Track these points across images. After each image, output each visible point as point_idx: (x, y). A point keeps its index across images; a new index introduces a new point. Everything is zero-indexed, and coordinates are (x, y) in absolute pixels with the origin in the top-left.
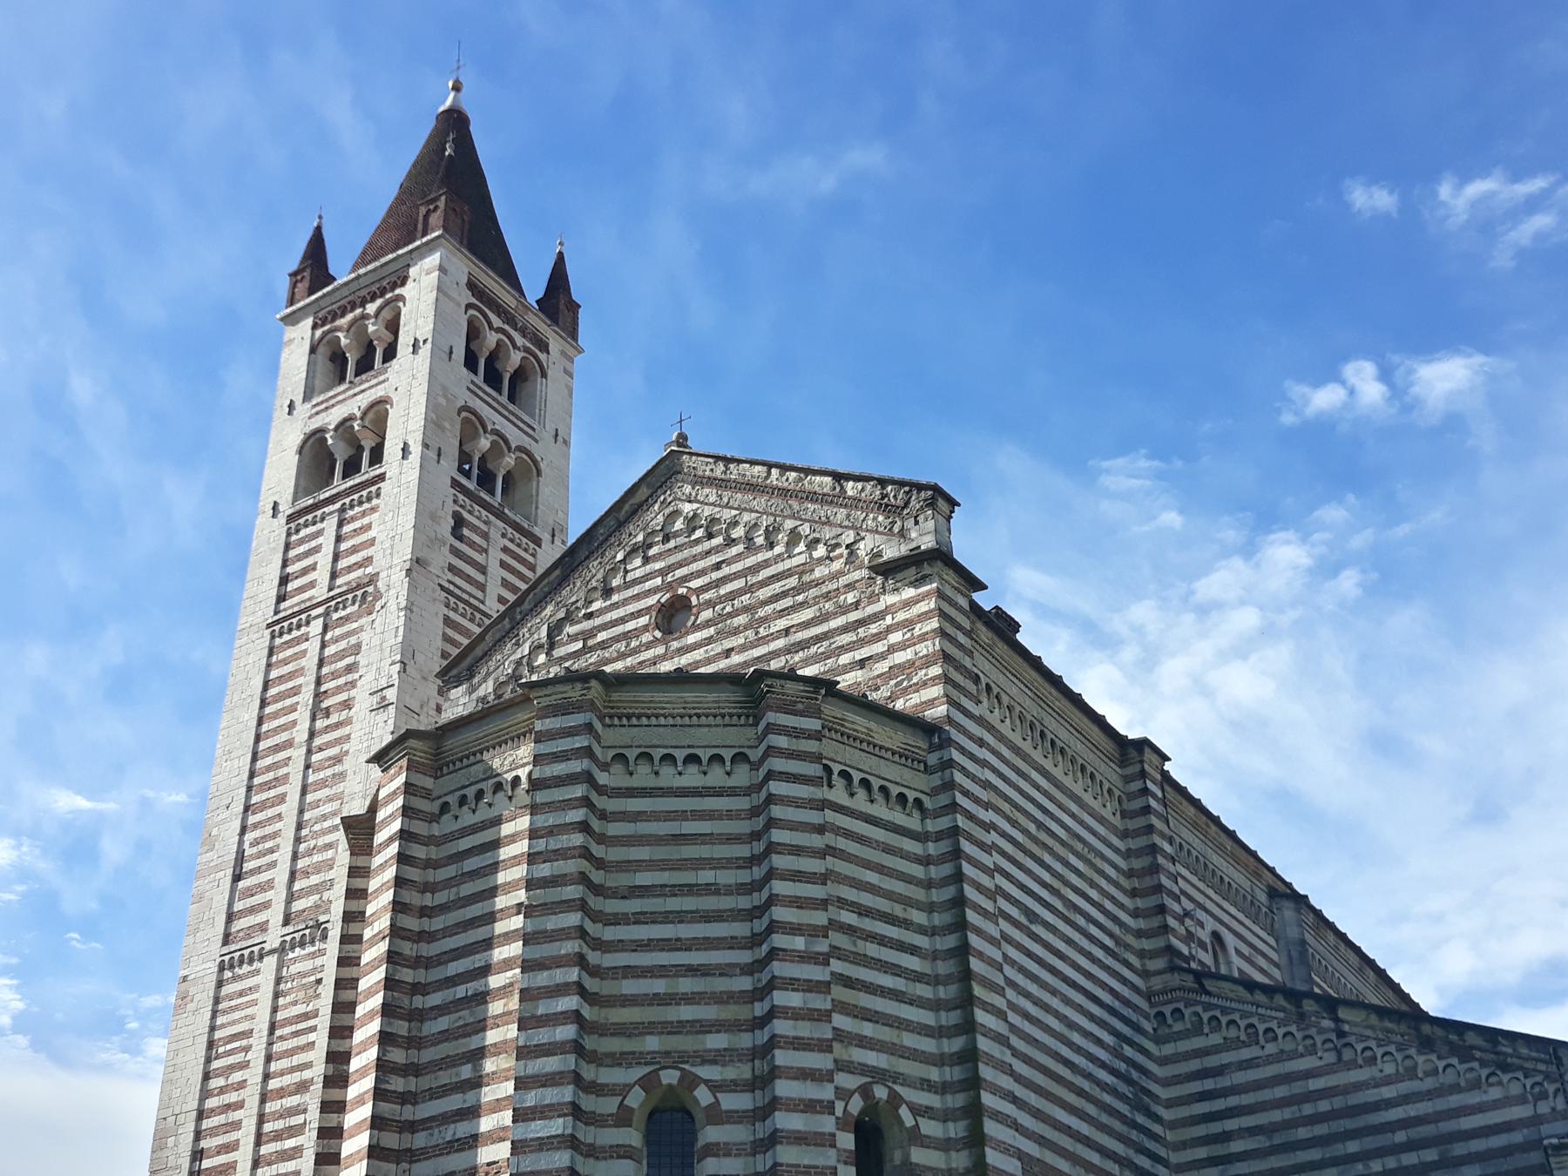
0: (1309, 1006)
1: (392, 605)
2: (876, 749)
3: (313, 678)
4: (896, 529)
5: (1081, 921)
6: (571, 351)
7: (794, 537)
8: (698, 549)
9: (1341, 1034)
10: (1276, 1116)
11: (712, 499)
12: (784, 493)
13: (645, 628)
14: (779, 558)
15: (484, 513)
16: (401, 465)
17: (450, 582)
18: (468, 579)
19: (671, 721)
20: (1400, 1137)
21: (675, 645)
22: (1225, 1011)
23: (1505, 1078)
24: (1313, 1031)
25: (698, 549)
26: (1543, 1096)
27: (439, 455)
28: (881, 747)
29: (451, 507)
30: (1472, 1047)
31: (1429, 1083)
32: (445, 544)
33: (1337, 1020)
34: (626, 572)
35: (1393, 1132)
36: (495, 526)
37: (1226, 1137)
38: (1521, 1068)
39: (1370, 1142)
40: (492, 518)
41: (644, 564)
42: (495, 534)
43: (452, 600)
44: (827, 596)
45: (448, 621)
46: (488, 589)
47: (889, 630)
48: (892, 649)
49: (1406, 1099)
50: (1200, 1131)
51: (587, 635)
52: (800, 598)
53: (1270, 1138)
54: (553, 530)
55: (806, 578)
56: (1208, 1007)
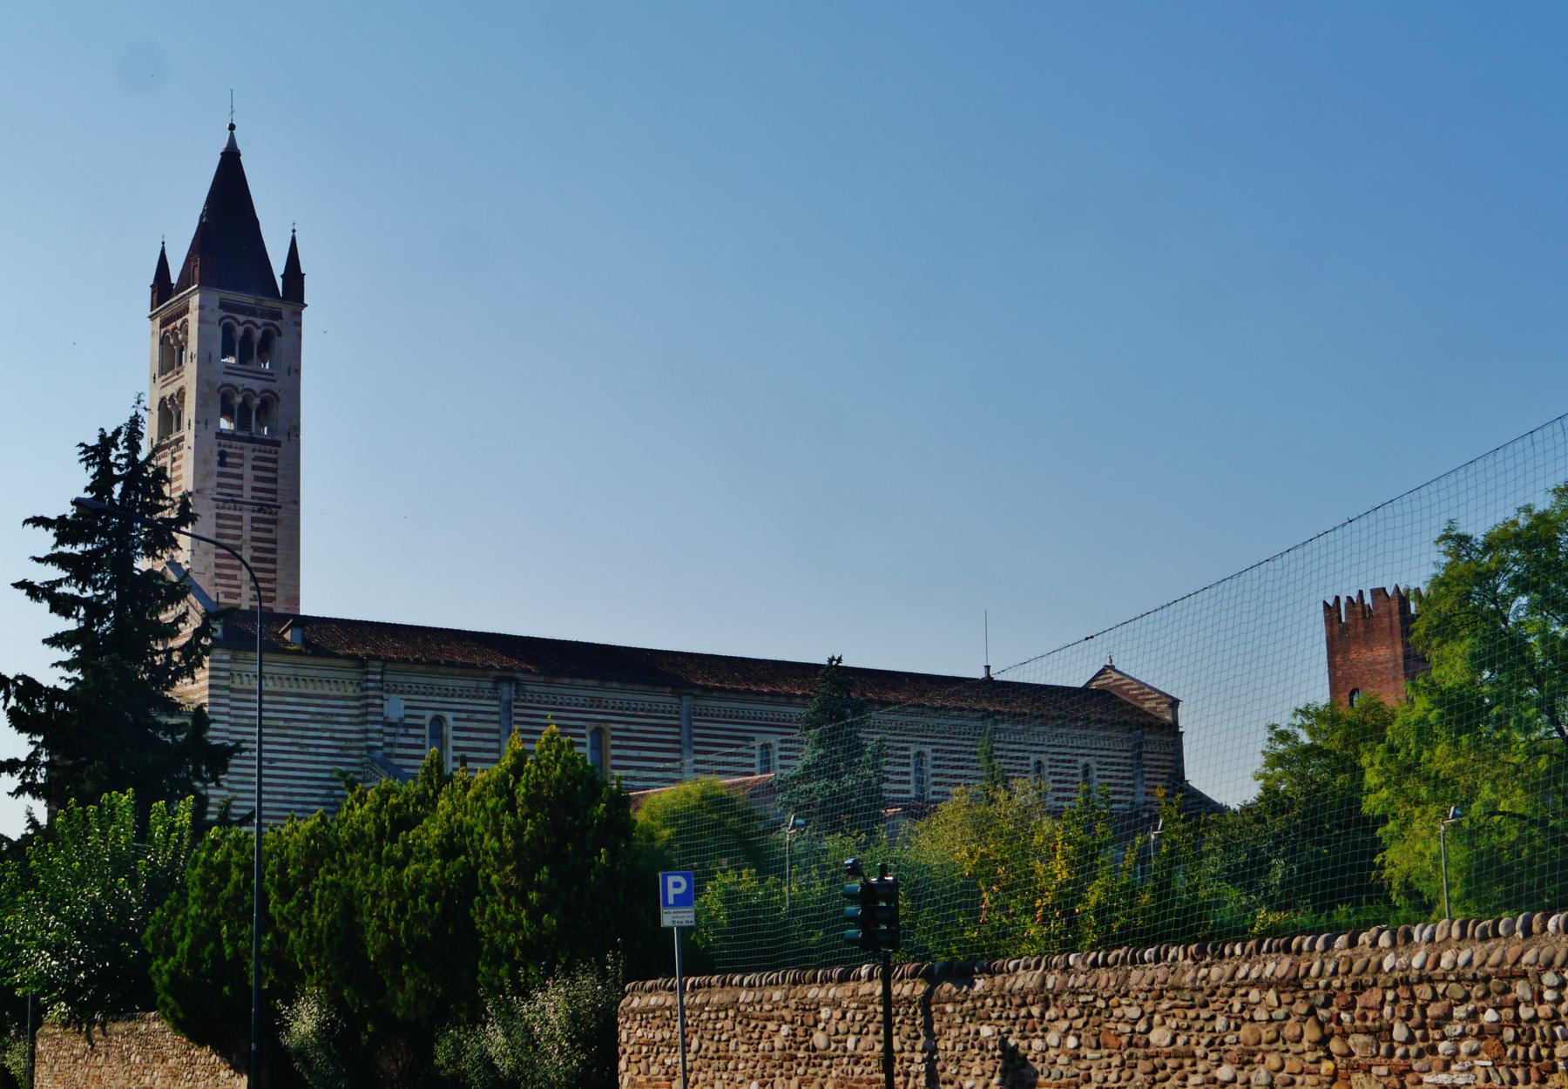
17: (218, 494)
27: (206, 424)
29: (216, 449)
40: (245, 444)
43: (221, 504)
45: (219, 516)
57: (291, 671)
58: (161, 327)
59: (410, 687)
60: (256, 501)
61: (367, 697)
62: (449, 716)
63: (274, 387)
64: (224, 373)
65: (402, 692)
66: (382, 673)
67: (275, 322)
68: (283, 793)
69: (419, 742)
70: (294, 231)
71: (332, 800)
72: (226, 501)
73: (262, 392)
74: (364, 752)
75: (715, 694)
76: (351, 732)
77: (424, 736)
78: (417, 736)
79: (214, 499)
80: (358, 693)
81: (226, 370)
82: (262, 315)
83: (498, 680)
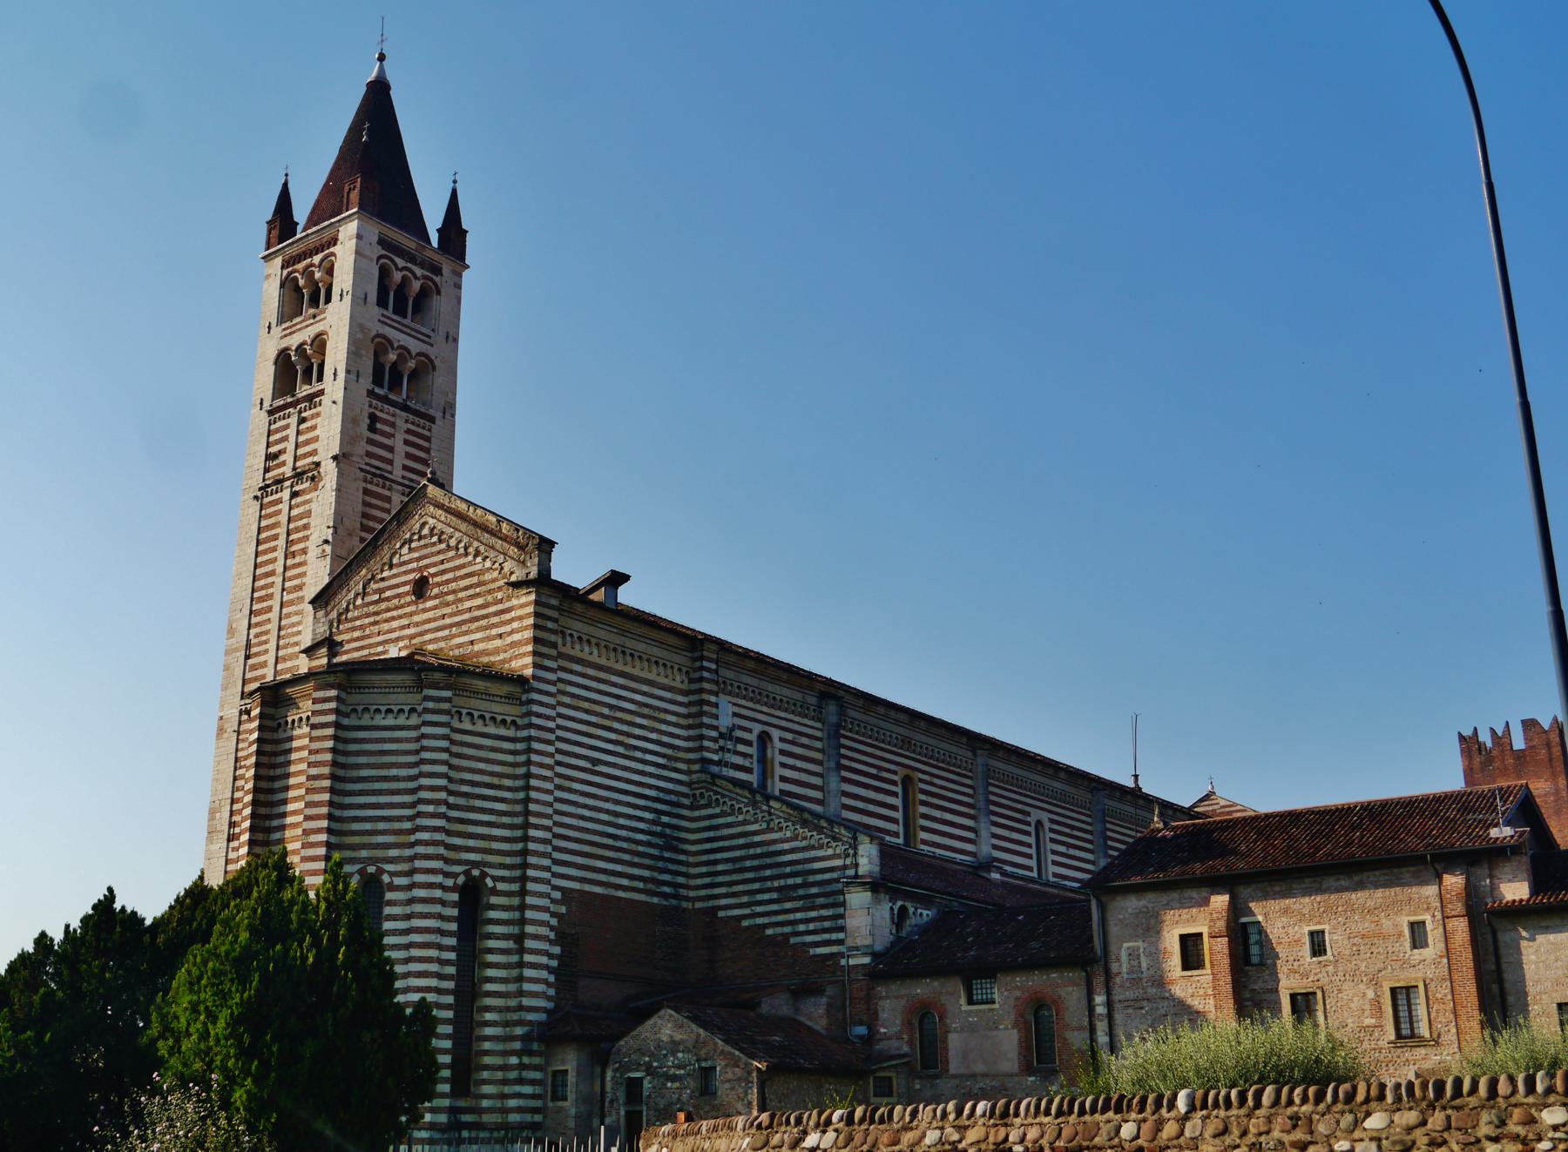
0: (758, 798)
1: (328, 486)
2: (490, 697)
3: (284, 530)
4: (522, 559)
5: (639, 755)
6: (458, 268)
7: (477, 554)
8: (435, 549)
9: (770, 814)
10: (738, 853)
11: (443, 519)
12: (475, 524)
13: (407, 593)
14: (470, 564)
15: (392, 409)
16: (333, 385)
17: (367, 464)
18: (381, 459)
19: (379, 690)
20: (788, 870)
21: (421, 606)
22: (723, 796)
23: (834, 844)
24: (758, 811)
25: (435, 549)
26: (847, 856)
27: (358, 376)
28: (493, 695)
29: (367, 410)
30: (823, 827)
31: (804, 843)
32: (363, 439)
33: (769, 806)
34: (401, 555)
35: (786, 867)
36: (400, 417)
37: (716, 862)
38: (841, 840)
39: (775, 871)
40: (398, 411)
41: (409, 553)
42: (400, 423)
43: (369, 476)
44: (489, 592)
45: (366, 492)
46: (395, 464)
47: (513, 620)
48: (512, 632)
49: (793, 851)
50: (705, 858)
51: (381, 591)
52: (478, 590)
53: (734, 865)
54: (444, 408)
55: (482, 578)
56: (716, 793)
57: (618, 640)
58: (282, 268)
59: (739, 687)
60: (407, 482)
61: (702, 691)
62: (776, 734)
63: (432, 352)
64: (379, 321)
65: (730, 694)
66: (717, 662)
67: (434, 277)
68: (607, 812)
69: (747, 764)
70: (455, 182)
71: (659, 829)
72: (374, 475)
73: (419, 354)
74: (696, 767)
75: (1001, 754)
76: (678, 737)
77: (751, 756)
78: (745, 755)
79: (362, 470)
80: (685, 687)
81: (382, 319)
82: (422, 265)
83: (823, 696)
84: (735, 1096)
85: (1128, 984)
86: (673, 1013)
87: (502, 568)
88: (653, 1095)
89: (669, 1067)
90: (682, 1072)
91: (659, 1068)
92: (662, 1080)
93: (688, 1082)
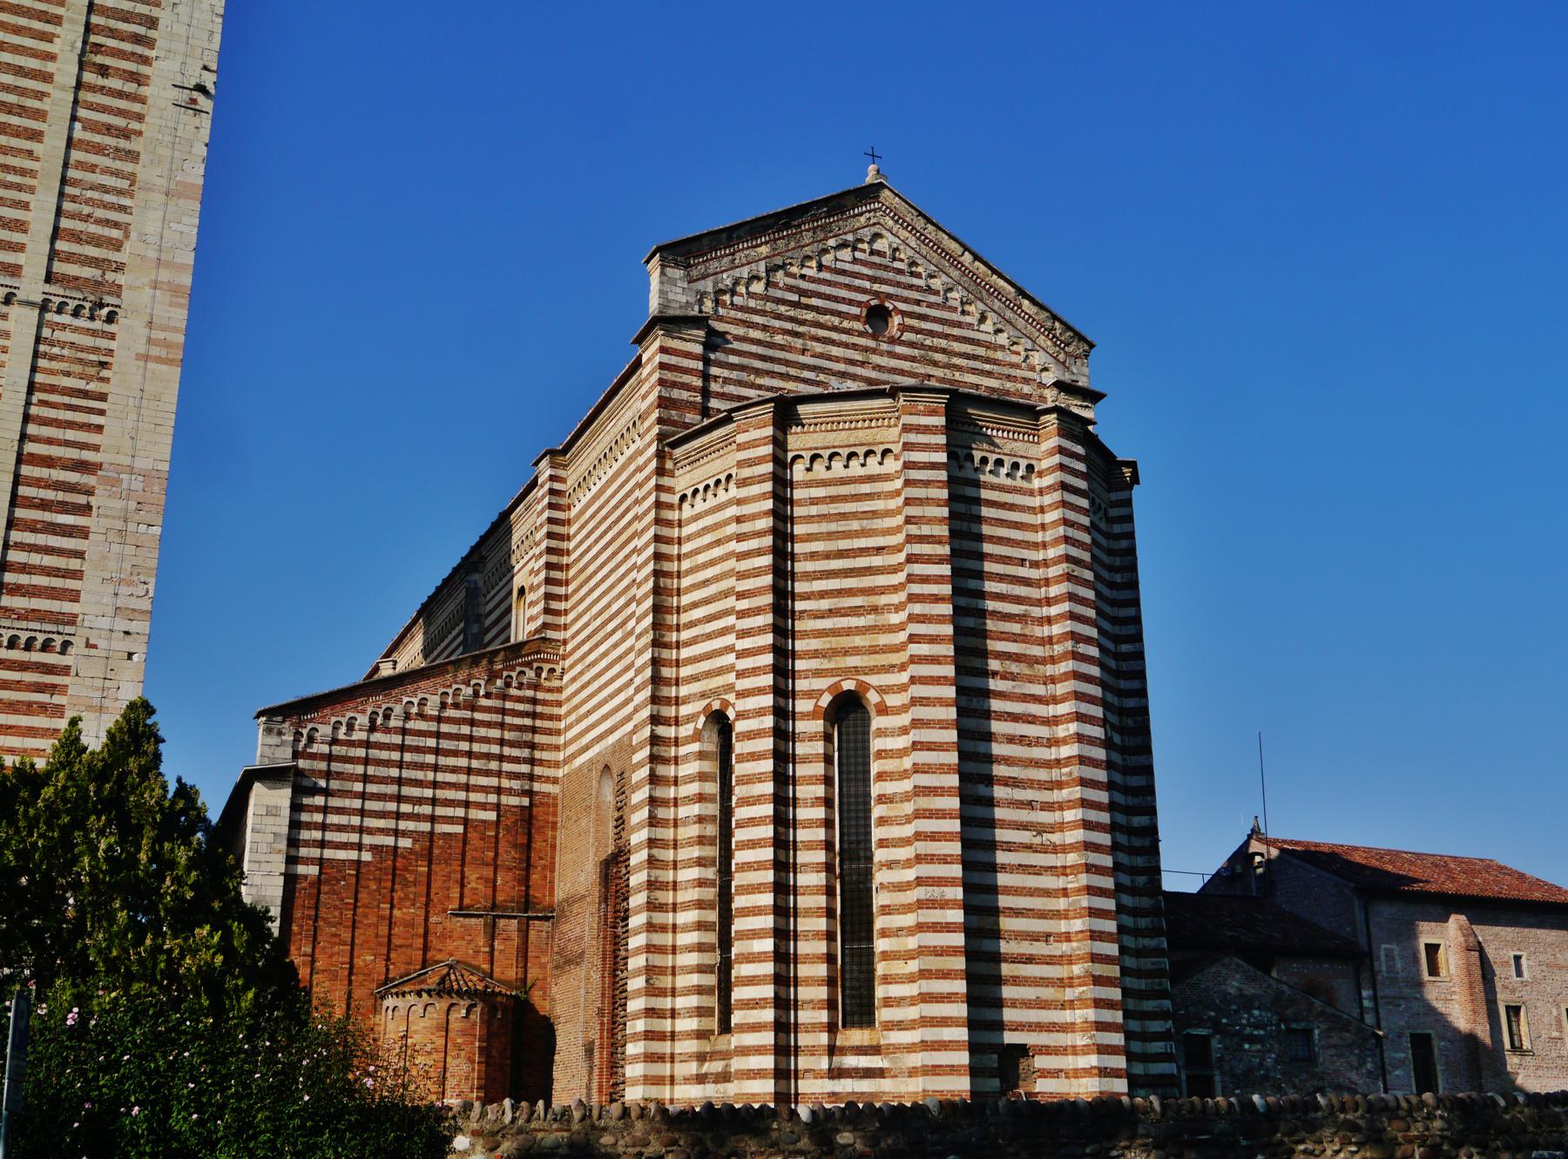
11: (913, 244)
13: (856, 318)
52: (987, 367)
84: (1345, 1065)
85: (1387, 983)
86: (1241, 962)
87: (1027, 357)
88: (1227, 1058)
89: (1243, 1026)
90: (1262, 1032)
91: (1230, 1025)
92: (1235, 1040)
93: (1271, 1045)
